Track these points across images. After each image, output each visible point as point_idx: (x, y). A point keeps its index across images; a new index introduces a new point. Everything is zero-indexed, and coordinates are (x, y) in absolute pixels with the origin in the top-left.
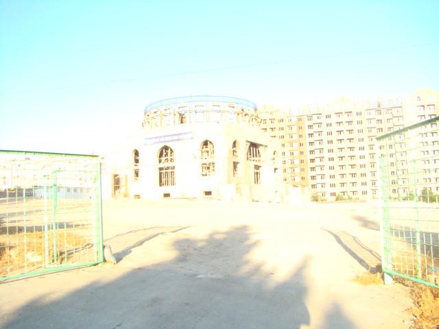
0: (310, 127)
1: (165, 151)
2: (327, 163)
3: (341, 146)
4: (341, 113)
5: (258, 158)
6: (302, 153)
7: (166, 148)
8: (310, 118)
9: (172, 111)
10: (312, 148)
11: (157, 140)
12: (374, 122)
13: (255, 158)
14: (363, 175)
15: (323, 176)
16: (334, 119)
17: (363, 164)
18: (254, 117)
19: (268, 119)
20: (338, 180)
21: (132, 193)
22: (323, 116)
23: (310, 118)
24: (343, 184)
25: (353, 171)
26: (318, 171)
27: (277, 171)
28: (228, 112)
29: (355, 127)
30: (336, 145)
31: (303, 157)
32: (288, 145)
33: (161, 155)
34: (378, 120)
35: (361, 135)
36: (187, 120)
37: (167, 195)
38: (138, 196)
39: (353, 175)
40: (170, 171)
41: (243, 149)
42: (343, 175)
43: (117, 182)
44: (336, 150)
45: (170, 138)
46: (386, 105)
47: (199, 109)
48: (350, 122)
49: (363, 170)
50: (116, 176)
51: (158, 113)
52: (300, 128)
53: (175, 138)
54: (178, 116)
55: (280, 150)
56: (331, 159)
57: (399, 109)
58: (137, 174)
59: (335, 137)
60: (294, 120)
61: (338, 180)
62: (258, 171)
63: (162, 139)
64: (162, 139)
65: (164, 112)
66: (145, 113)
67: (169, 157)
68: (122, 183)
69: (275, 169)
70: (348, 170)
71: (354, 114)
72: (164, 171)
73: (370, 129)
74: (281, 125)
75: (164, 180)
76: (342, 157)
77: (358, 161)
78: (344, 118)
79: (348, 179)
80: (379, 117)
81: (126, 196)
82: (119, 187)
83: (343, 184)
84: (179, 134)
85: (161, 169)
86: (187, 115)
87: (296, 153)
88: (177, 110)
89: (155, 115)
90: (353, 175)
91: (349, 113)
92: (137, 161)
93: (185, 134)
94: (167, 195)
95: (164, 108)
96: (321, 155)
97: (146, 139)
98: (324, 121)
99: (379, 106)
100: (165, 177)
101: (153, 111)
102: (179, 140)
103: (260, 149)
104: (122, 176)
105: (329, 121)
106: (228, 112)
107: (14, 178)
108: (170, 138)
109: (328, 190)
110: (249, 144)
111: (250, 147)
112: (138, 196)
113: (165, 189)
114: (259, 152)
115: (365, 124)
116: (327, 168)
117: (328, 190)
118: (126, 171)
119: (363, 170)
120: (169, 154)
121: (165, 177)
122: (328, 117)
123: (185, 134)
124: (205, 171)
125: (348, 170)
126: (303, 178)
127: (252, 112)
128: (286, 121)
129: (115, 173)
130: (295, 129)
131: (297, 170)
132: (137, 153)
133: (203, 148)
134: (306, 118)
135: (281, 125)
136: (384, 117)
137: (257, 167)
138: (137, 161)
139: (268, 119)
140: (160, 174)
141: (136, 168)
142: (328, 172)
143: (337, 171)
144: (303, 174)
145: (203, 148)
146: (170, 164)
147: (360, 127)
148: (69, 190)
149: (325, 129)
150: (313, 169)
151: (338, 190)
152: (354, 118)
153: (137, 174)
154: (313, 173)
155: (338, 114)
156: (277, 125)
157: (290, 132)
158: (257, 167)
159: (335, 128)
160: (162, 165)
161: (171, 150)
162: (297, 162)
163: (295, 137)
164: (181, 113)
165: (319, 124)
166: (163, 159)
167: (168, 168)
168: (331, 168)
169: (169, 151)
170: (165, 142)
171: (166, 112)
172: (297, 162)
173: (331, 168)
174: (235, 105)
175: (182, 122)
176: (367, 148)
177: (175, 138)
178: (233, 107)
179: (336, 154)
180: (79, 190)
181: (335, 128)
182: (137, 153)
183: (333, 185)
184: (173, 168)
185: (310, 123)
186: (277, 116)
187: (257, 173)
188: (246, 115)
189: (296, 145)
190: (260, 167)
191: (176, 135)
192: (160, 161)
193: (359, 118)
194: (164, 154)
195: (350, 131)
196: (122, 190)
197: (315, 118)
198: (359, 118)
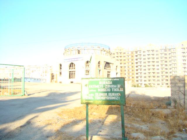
0: (136, 56)
1: (72, 65)
2: (143, 72)
3: (149, 64)
4: (150, 51)
5: (109, 68)
6: (133, 67)
7: (72, 63)
8: (136, 52)
9: (75, 48)
10: (137, 65)
11: (69, 60)
12: (163, 55)
13: (108, 68)
14: (158, 77)
15: (141, 77)
16: (147, 53)
17: (145, 69)
18: (108, 52)
19: (119, 52)
20: (147, 79)
21: (59, 81)
22: (142, 52)
23: (136, 52)
24: (149, 80)
25: (154, 75)
26: (139, 74)
27: (117, 74)
28: (97, 50)
29: (155, 56)
30: (147, 64)
31: (133, 69)
32: (127, 63)
33: (70, 66)
34: (165, 54)
35: (157, 60)
36: (81, 53)
37: (72, 82)
38: (61, 82)
39: (154, 77)
40: (73, 73)
41: (103, 65)
42: (149, 77)
43: (53, 77)
44: (147, 66)
45: (74, 60)
46: (169, 48)
47: (85, 48)
48: (153, 55)
49: (158, 75)
50: (52, 74)
51: (70, 50)
52: (132, 56)
53: (76, 59)
54: (77, 51)
55: (119, 66)
56: (145, 70)
57: (174, 49)
58: (61, 73)
59: (147, 60)
60: (130, 53)
61: (147, 79)
62: (109, 74)
63: (71, 60)
64: (71, 60)
65: (72, 49)
66: (65, 49)
67: (73, 67)
68: (55, 77)
69: (117, 73)
70: (152, 75)
71: (155, 51)
72: (71, 73)
73: (161, 58)
74: (124, 55)
75: (71, 76)
76: (149, 69)
77: (156, 71)
78: (151, 53)
79: (152, 78)
80: (165, 53)
81: (56, 82)
82: (53, 79)
83: (149, 80)
84: (77, 58)
85: (70, 72)
86: (81, 51)
87: (130, 67)
88: (77, 49)
89: (68, 50)
90: (154, 77)
91: (153, 51)
92: (61, 68)
93: (80, 58)
94: (72, 82)
95: (72, 47)
96: (141, 68)
97: (65, 60)
98: (142, 53)
99: (166, 48)
100: (71, 75)
101: (68, 49)
102: (77, 60)
103: (111, 65)
104: (55, 74)
105: (144, 54)
106: (97, 50)
107: (16, 74)
108: (74, 60)
109: (143, 83)
110: (105, 63)
111: (106, 64)
112: (61, 82)
113: (71, 80)
114: (110, 66)
115: (160, 55)
116: (143, 73)
117: (143, 83)
118: (56, 71)
119: (158, 75)
120: (73, 66)
121: (71, 75)
122: (144, 52)
123: (80, 58)
124: (87, 73)
125: (152, 75)
126: (133, 77)
127: (108, 50)
128: (126, 53)
129: (52, 73)
130: (130, 57)
131: (130, 74)
132: (61, 65)
133: (86, 64)
134: (135, 52)
135: (124, 55)
136: (168, 52)
137: (109, 72)
138: (61, 68)
139: (119, 52)
140: (70, 74)
141: (60, 71)
142: (143, 75)
143: (147, 75)
144: (133, 76)
145: (86, 64)
146: (73, 70)
147: (157, 56)
148: (35, 79)
149: (142, 57)
150: (137, 74)
151: (147, 83)
152: (155, 53)
153: (61, 73)
154: (137, 76)
155: (148, 51)
156: (122, 55)
157: (128, 58)
158: (109, 72)
159: (147, 57)
160: (71, 70)
161: (74, 64)
162: (130, 70)
163: (130, 60)
164: (79, 50)
165: (140, 55)
166: (71, 68)
167: (73, 71)
168: (145, 73)
169: (73, 65)
170: (72, 61)
171: (73, 49)
172: (130, 70)
173: (145, 73)
174: (100, 47)
175: (79, 53)
176: (160, 65)
177: (76, 59)
178: (100, 48)
179: (147, 68)
180: (39, 80)
181: (147, 57)
182: (61, 65)
183: (145, 81)
184: (75, 71)
185: (137, 54)
186: (123, 51)
187: (109, 74)
188: (104, 51)
189: (130, 64)
190: (110, 72)
191: (74, 59)
192: (70, 69)
193: (157, 53)
194: (72, 66)
195: (153, 58)
196: (55, 80)
197: (138, 52)
198: (157, 53)
